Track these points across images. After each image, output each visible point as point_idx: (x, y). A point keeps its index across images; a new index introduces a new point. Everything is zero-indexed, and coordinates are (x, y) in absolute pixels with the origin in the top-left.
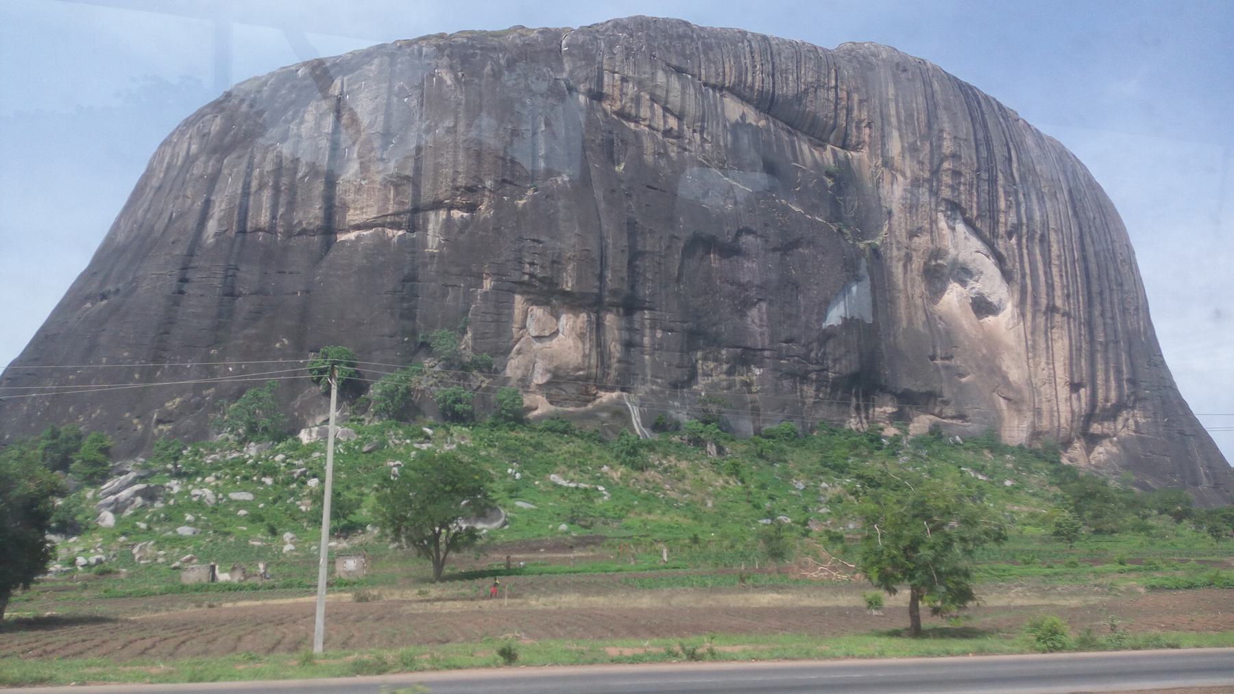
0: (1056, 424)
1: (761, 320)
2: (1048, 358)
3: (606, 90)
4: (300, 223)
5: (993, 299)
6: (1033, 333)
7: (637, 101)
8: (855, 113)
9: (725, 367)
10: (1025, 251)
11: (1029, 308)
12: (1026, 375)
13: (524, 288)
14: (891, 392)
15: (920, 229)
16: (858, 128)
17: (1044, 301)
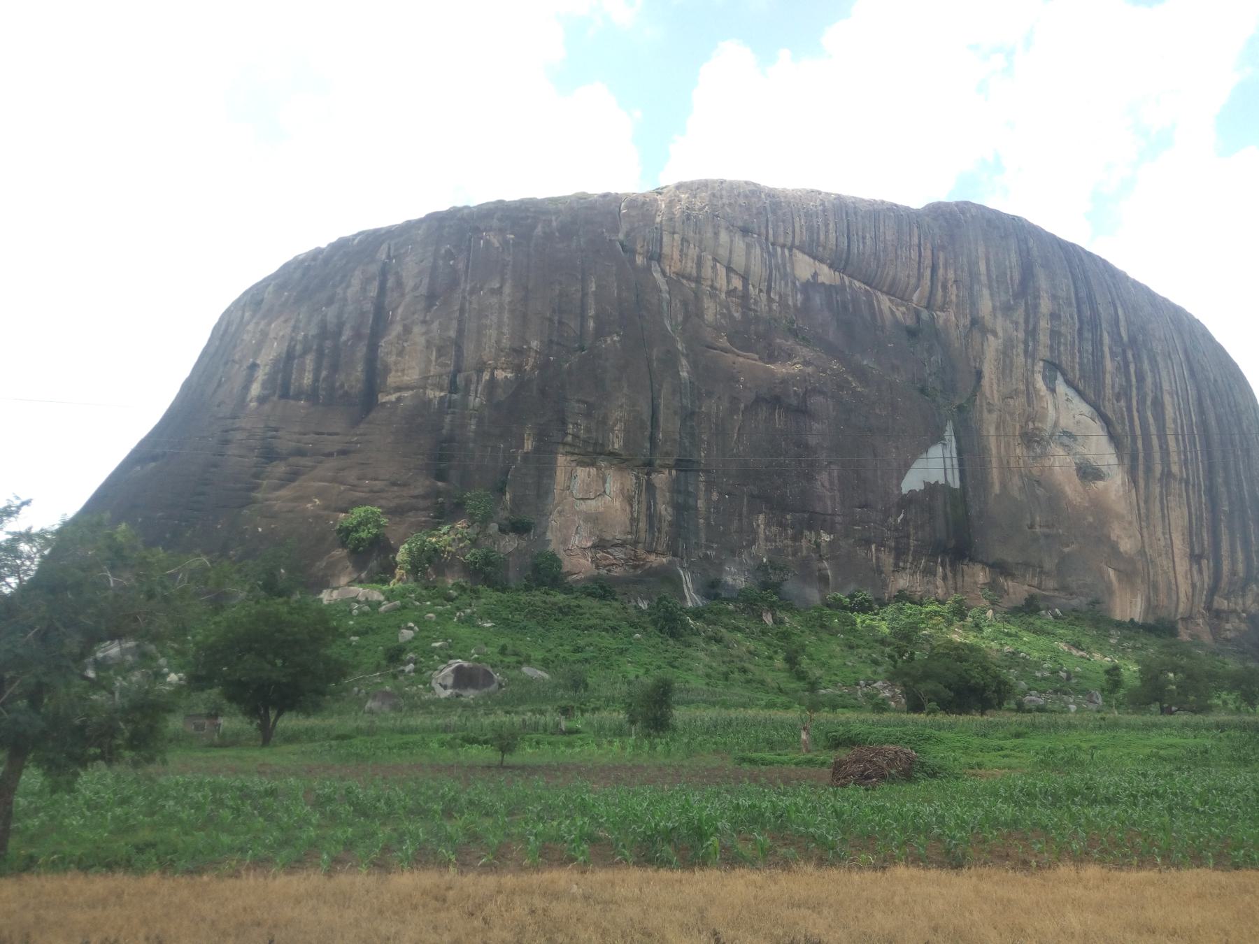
0: (1175, 598)
1: (831, 483)
2: (1164, 528)
3: (666, 250)
4: (342, 386)
6: (1146, 502)
7: (699, 263)
8: (941, 271)
9: (790, 532)
10: (1135, 414)
11: (1141, 473)
13: (568, 449)
14: (981, 562)
16: (945, 287)
17: (1158, 469)
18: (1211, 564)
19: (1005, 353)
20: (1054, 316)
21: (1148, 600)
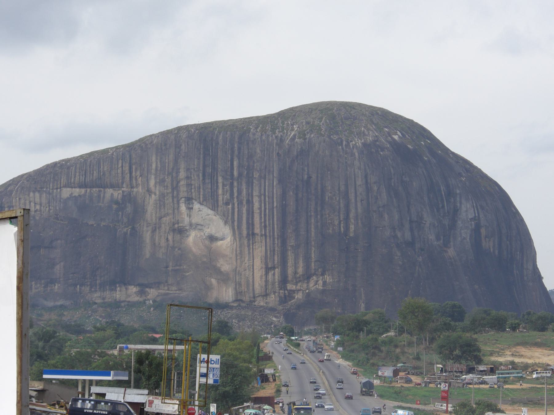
0: (251, 288)
3: (14, 204)
5: (219, 235)
8: (134, 173)
10: (236, 210)
11: (237, 236)
12: (234, 267)
15: (168, 214)
16: (136, 179)
18: (279, 271)
19: (160, 200)
20: (188, 178)
21: (236, 289)
